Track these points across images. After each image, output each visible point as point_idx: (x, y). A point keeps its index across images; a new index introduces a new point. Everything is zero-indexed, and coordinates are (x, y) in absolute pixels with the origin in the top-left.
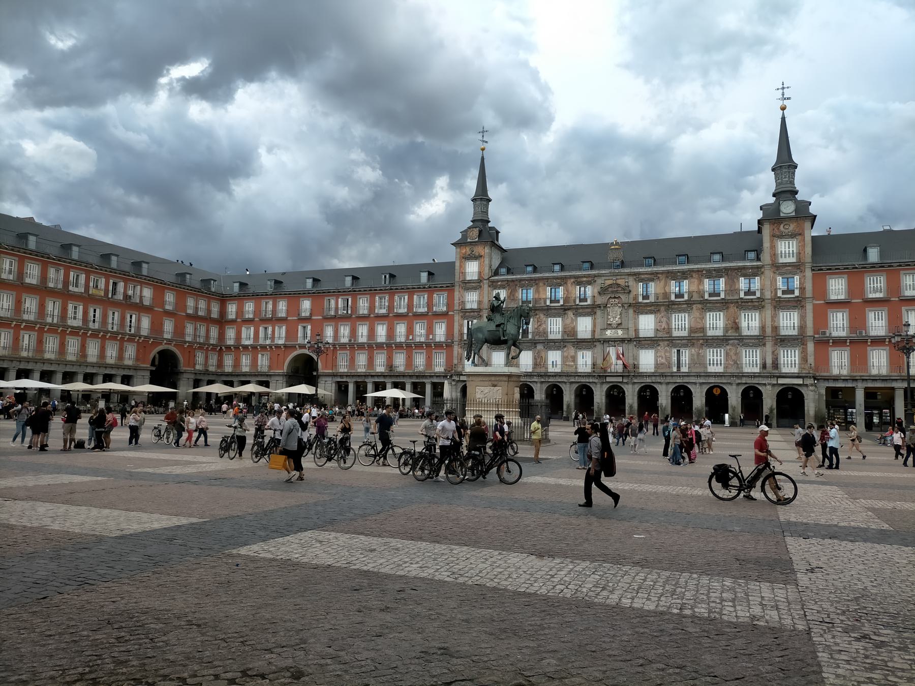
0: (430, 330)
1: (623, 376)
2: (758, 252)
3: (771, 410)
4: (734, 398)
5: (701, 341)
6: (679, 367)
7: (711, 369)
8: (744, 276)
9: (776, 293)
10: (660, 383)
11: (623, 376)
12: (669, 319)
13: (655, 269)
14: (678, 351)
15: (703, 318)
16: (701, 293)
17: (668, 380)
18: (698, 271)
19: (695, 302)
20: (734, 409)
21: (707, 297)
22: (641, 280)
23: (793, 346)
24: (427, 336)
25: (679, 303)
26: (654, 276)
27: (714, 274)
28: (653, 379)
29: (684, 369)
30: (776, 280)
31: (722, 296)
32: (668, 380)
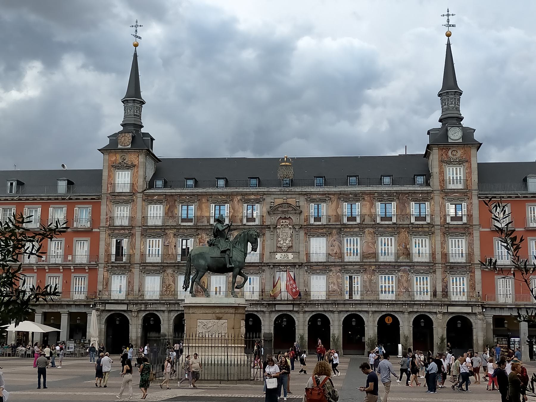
0: (69, 250)
1: (293, 304)
2: (428, 175)
3: (442, 340)
4: (406, 328)
5: (373, 267)
6: (351, 295)
7: (383, 297)
8: (415, 200)
9: (445, 220)
10: (332, 312)
11: (293, 304)
12: (341, 242)
13: (326, 189)
14: (351, 278)
15: (375, 243)
16: (373, 217)
17: (341, 308)
18: (371, 194)
19: (368, 226)
20: (406, 338)
21: (378, 220)
22: (313, 201)
23: (462, 274)
24: (65, 257)
25: (352, 227)
26: (325, 198)
27: (386, 198)
28: (326, 308)
29: (357, 297)
30: (445, 206)
31: (394, 220)
32: (341, 308)
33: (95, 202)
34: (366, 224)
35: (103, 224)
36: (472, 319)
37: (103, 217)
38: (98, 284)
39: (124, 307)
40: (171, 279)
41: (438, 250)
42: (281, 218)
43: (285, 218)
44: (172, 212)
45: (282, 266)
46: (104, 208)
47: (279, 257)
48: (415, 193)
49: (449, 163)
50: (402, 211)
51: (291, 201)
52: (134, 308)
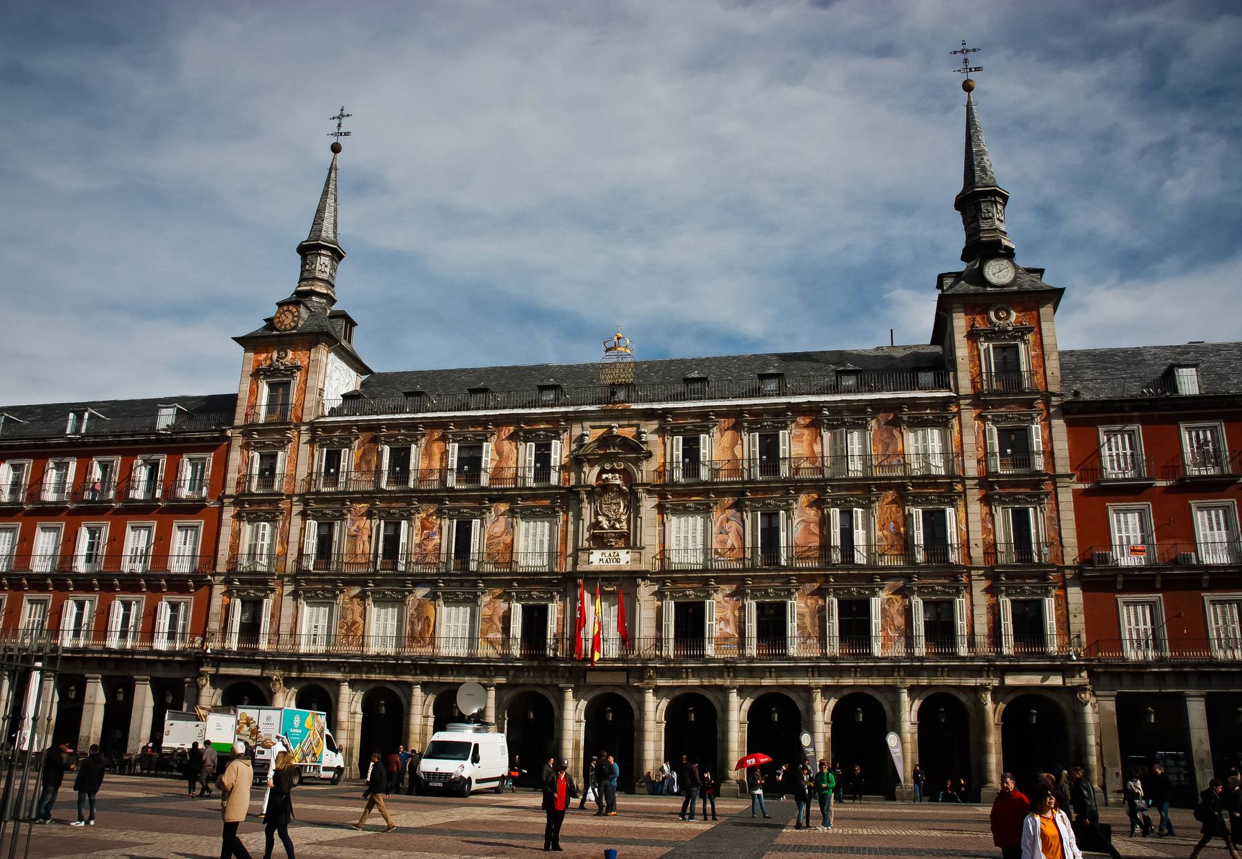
33: (219, 445)
34: (801, 481)
35: (231, 490)
36: (1063, 702)
37: (232, 476)
38: (211, 617)
39: (256, 672)
40: (358, 609)
41: (977, 535)
42: (603, 471)
43: (613, 471)
44: (368, 462)
45: (604, 579)
46: (236, 458)
47: (598, 560)
48: (912, 403)
49: (990, 335)
50: (887, 446)
51: (629, 433)
52: (276, 674)
